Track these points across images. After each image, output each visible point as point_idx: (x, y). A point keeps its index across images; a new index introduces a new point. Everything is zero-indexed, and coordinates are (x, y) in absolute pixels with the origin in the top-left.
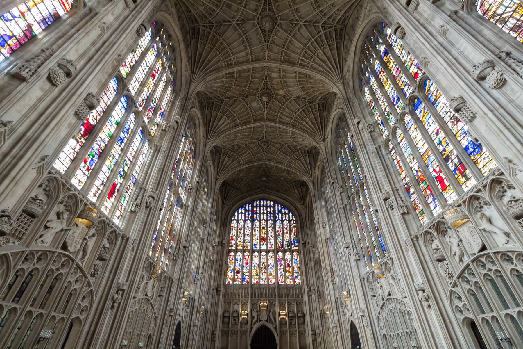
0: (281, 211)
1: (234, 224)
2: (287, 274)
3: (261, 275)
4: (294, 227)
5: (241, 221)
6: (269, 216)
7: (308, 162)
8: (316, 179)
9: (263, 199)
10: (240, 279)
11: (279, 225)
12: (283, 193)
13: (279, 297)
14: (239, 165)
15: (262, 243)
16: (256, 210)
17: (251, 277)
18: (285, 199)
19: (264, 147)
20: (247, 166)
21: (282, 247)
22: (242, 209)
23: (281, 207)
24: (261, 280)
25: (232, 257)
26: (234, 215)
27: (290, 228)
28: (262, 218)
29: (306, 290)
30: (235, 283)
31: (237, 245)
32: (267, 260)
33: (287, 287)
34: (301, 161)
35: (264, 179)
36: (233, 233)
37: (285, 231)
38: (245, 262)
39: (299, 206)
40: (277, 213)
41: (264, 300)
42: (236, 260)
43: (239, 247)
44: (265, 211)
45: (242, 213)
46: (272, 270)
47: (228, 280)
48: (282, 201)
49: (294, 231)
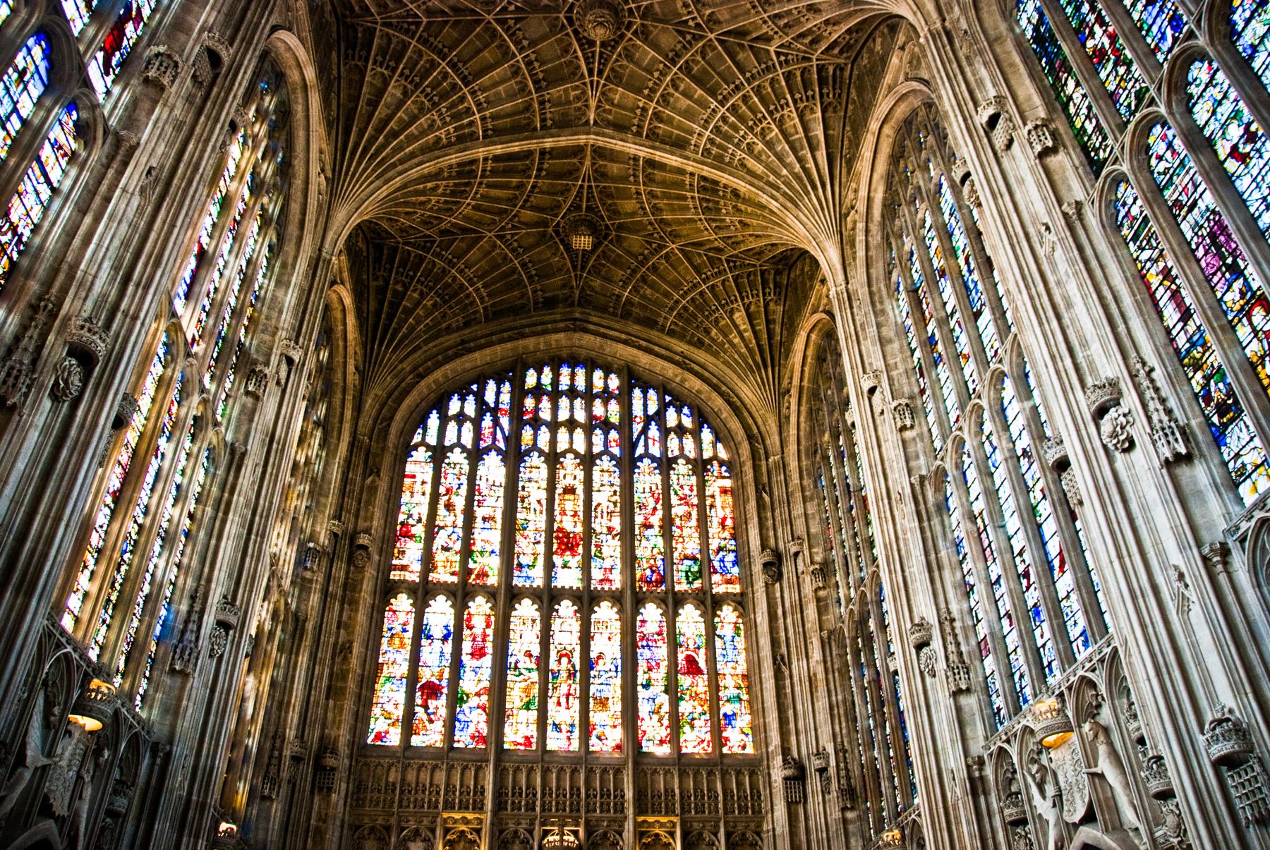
0: (660, 417)
1: (419, 466)
2: (685, 707)
3: (551, 704)
4: (724, 491)
5: (457, 456)
6: (598, 437)
7: (819, 132)
8: (861, 206)
9: (573, 362)
10: (439, 726)
11: (647, 479)
12: (671, 333)
13: (641, 809)
14: (461, 139)
15: (557, 560)
16: (537, 409)
17: (498, 714)
18: (684, 363)
19: (599, 34)
20: (499, 149)
21: (661, 581)
22: (463, 399)
23: (661, 400)
24: (550, 733)
25: (402, 617)
26: (423, 423)
27: (702, 495)
28: (562, 445)
29: (778, 774)
30: (416, 741)
31: (428, 561)
32: (586, 638)
33: (681, 762)
34: (780, 123)
35: (583, 242)
36: (414, 504)
37: (678, 510)
38: (467, 647)
39: (748, 392)
40: (637, 428)
41: (562, 825)
42: (421, 632)
43: (442, 575)
44: (580, 416)
45: (461, 418)
46: (608, 685)
47: (378, 724)
48: (671, 370)
49: (722, 509)
